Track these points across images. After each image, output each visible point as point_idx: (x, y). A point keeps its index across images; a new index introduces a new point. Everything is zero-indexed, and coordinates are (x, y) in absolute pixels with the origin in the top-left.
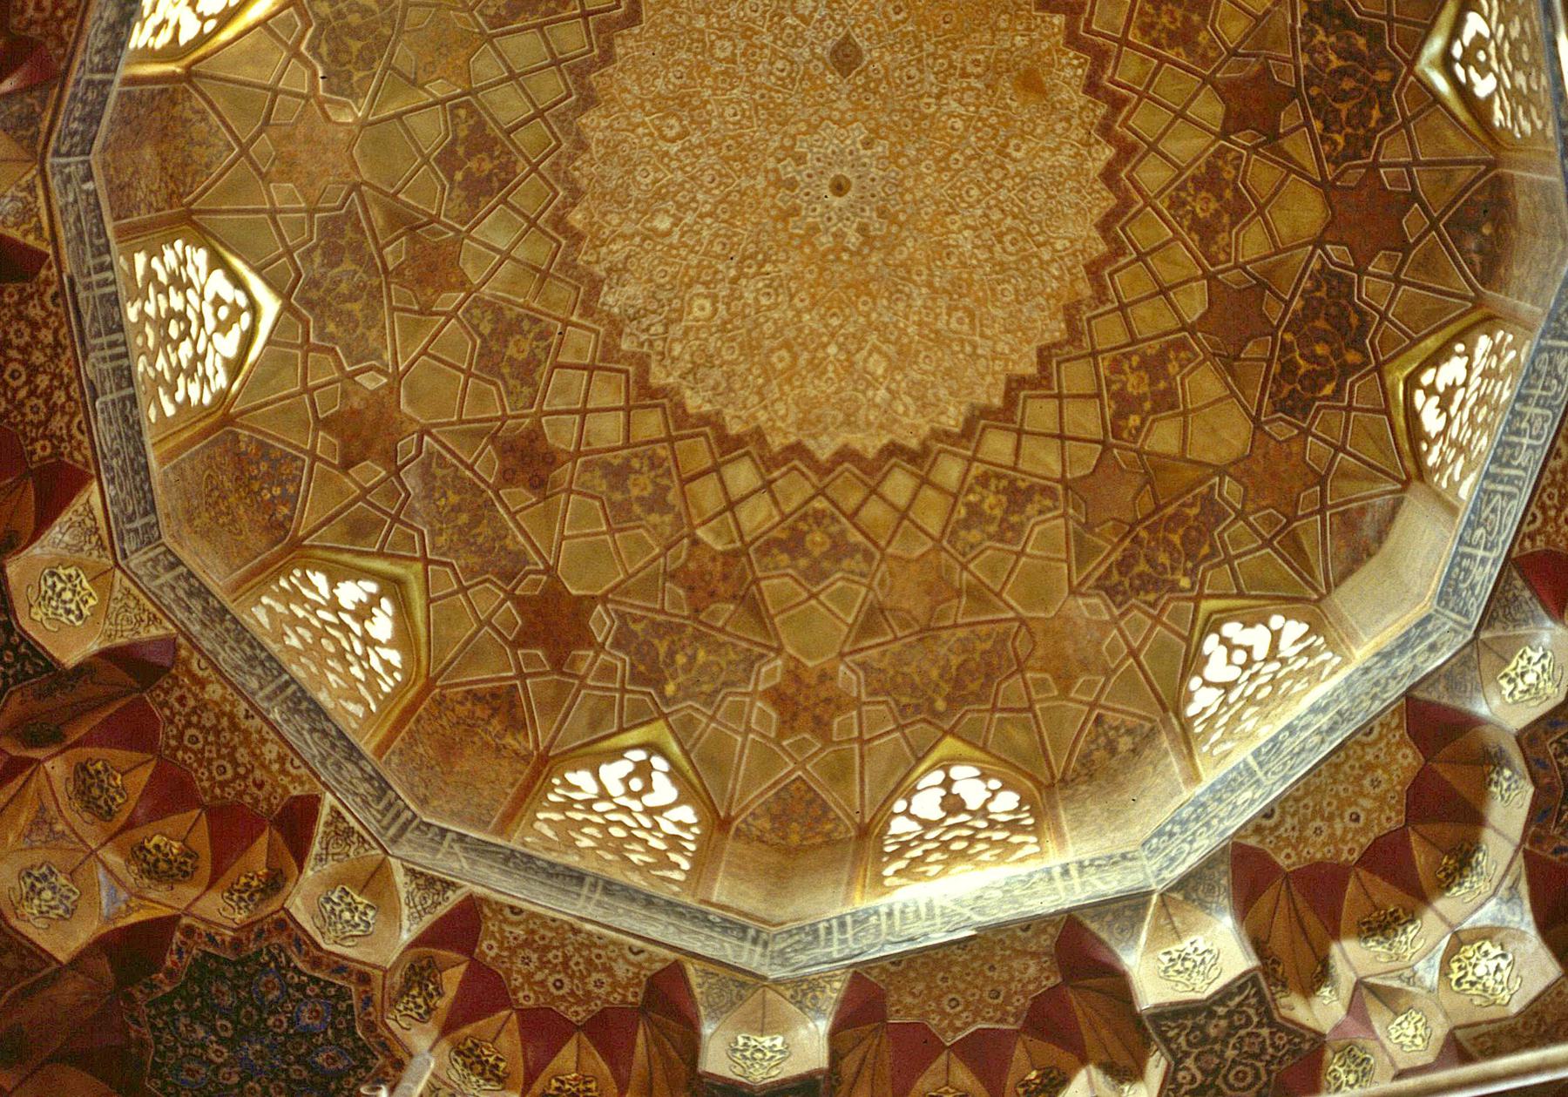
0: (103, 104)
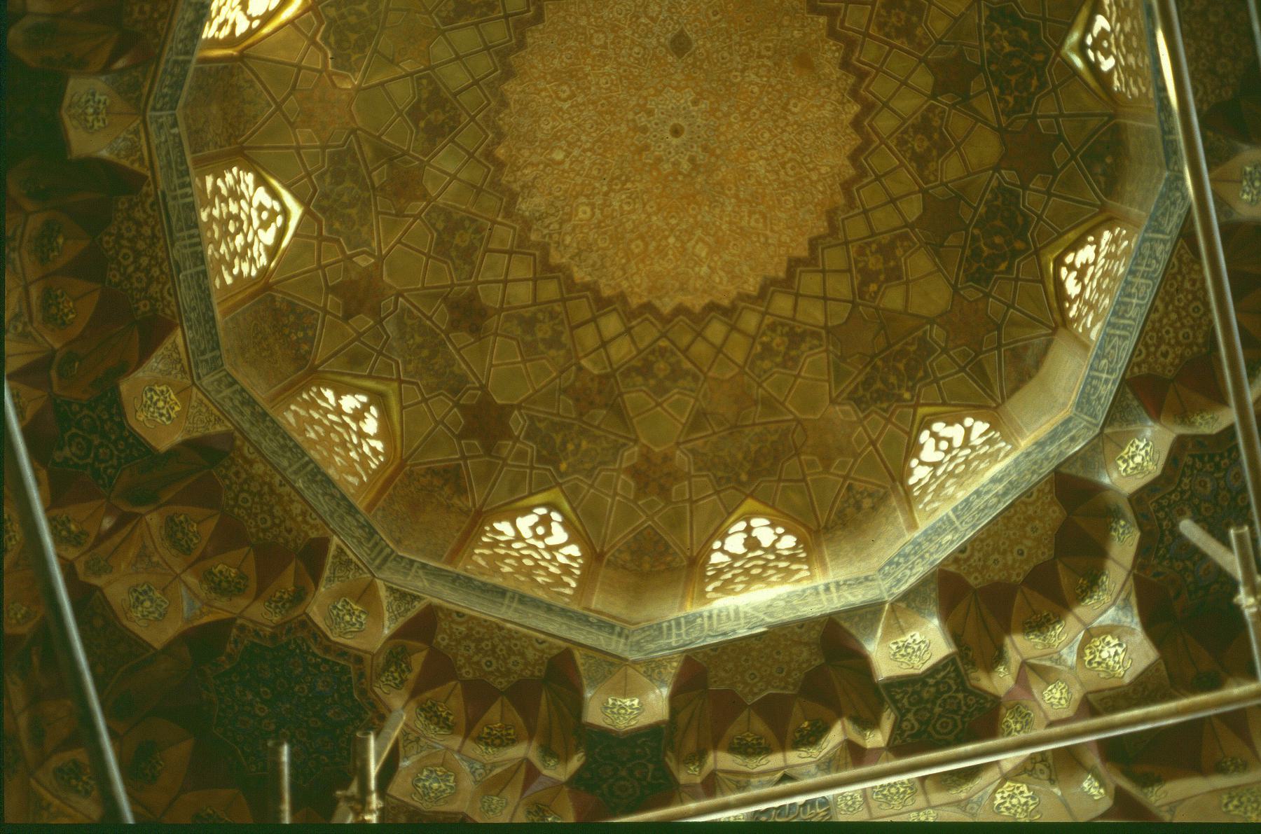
0: (185, 76)
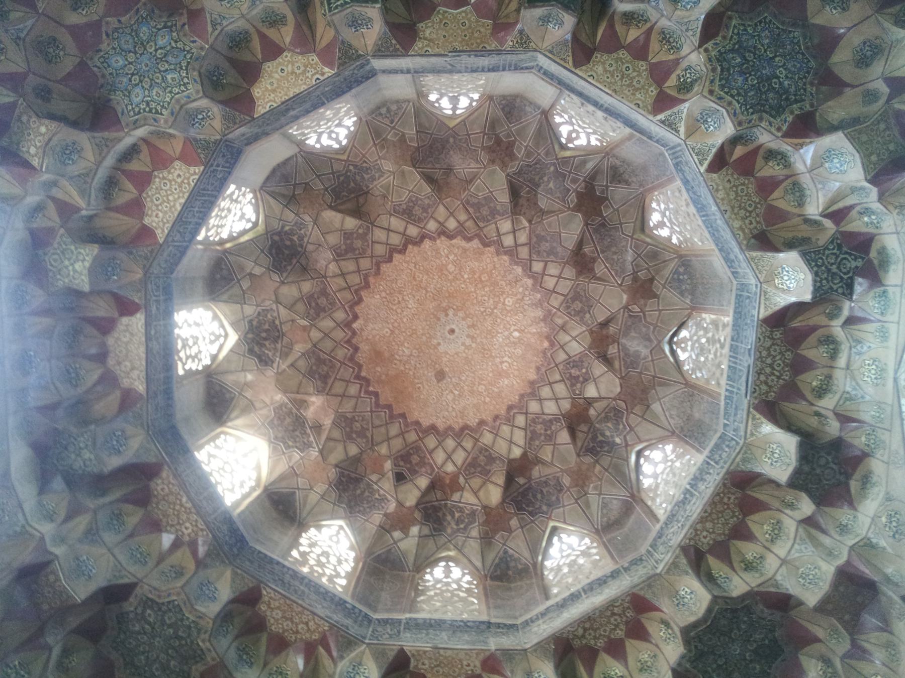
0: (712, 451)
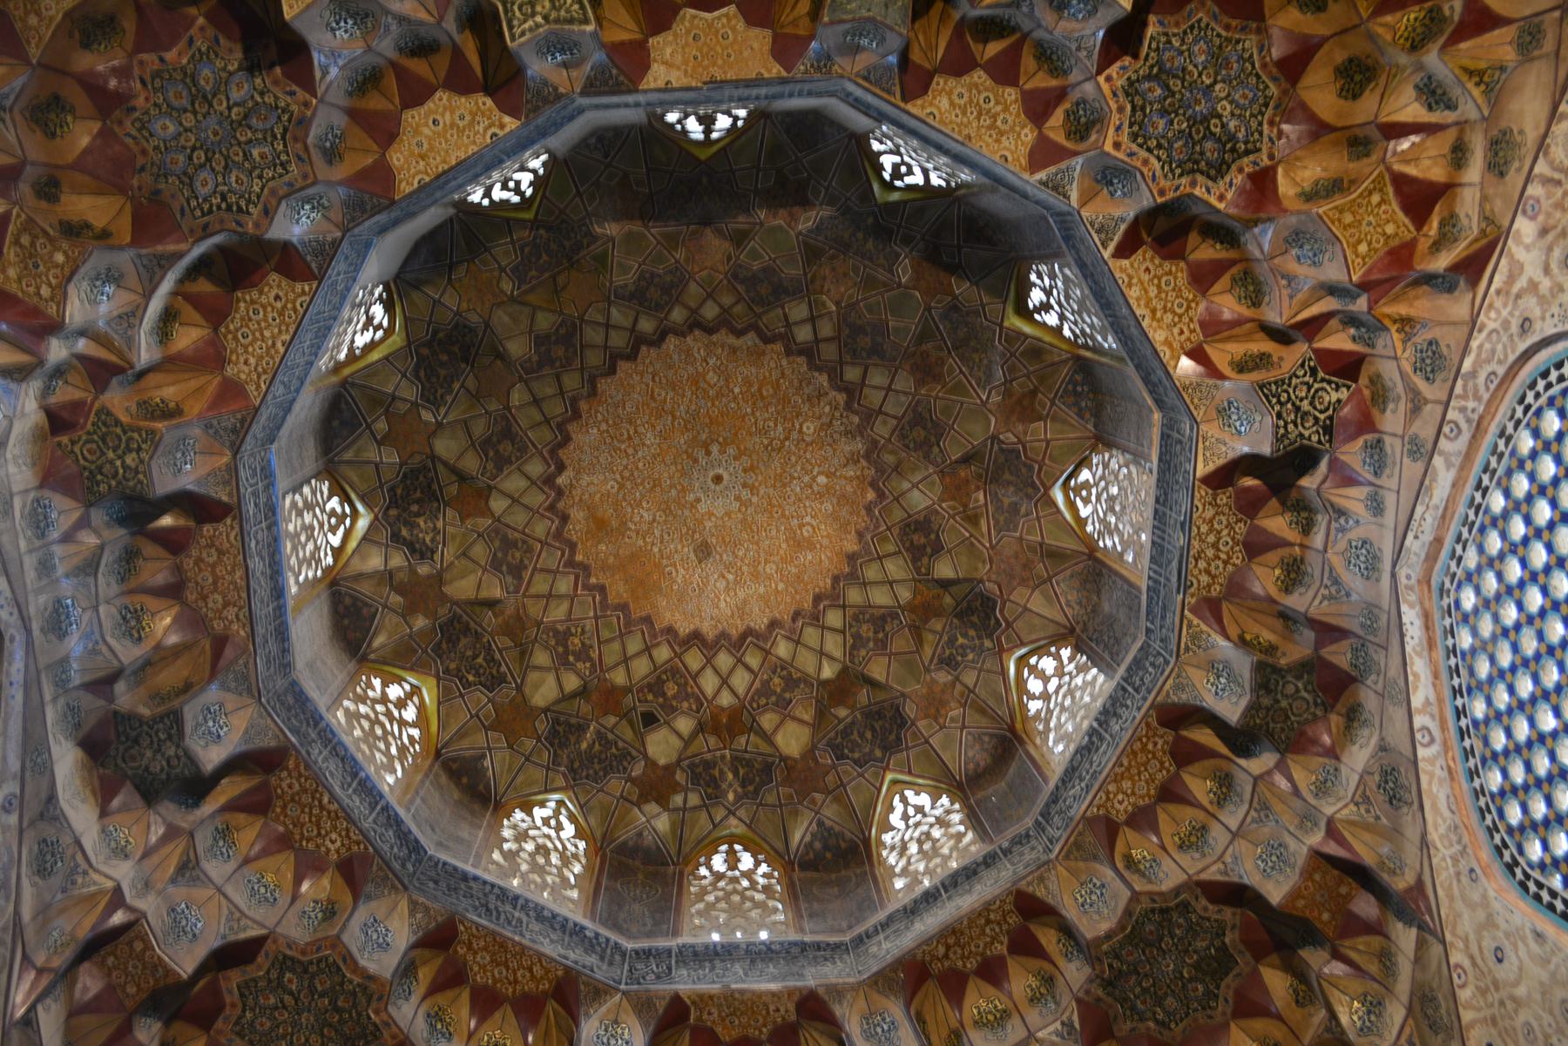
0: (1129, 669)
